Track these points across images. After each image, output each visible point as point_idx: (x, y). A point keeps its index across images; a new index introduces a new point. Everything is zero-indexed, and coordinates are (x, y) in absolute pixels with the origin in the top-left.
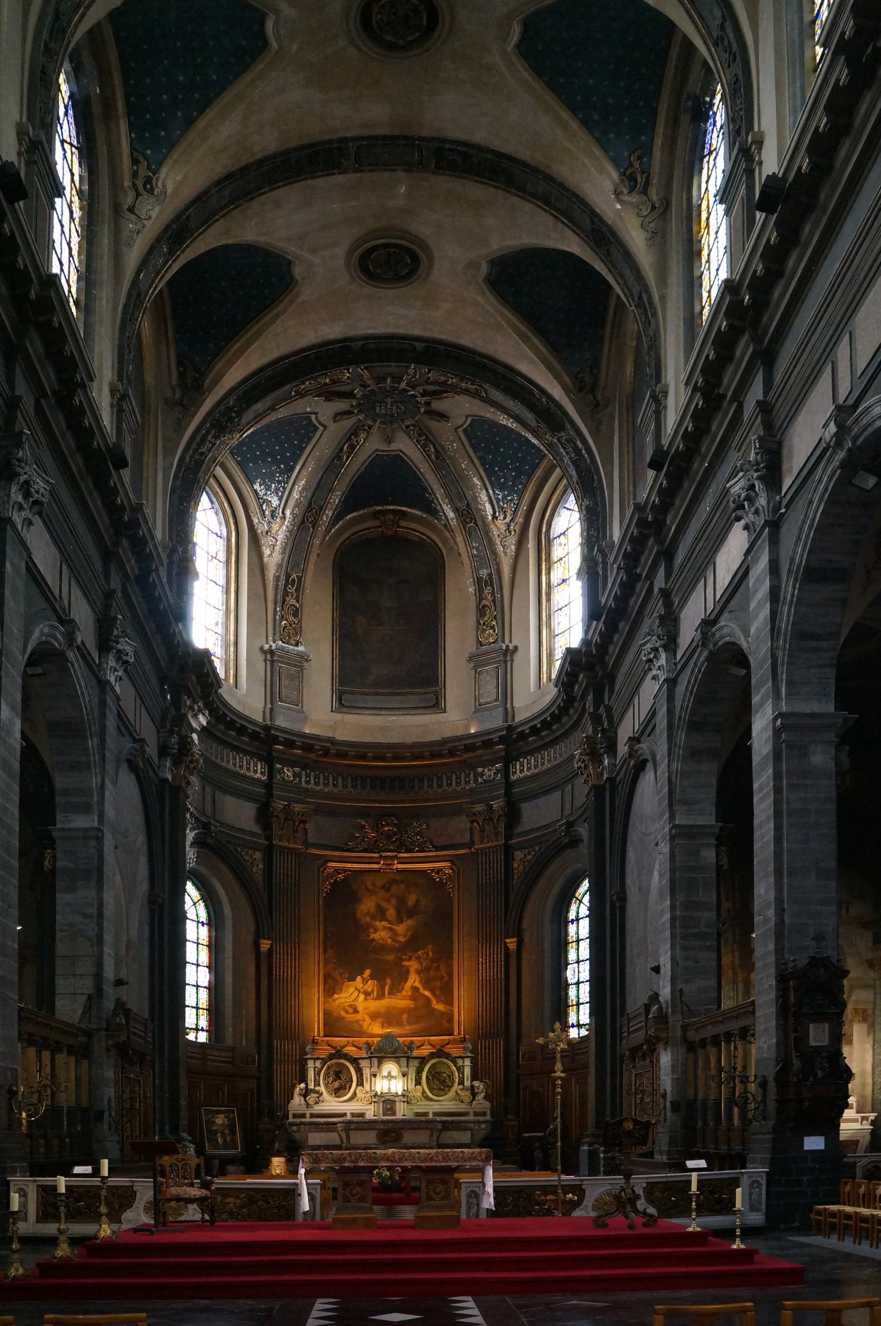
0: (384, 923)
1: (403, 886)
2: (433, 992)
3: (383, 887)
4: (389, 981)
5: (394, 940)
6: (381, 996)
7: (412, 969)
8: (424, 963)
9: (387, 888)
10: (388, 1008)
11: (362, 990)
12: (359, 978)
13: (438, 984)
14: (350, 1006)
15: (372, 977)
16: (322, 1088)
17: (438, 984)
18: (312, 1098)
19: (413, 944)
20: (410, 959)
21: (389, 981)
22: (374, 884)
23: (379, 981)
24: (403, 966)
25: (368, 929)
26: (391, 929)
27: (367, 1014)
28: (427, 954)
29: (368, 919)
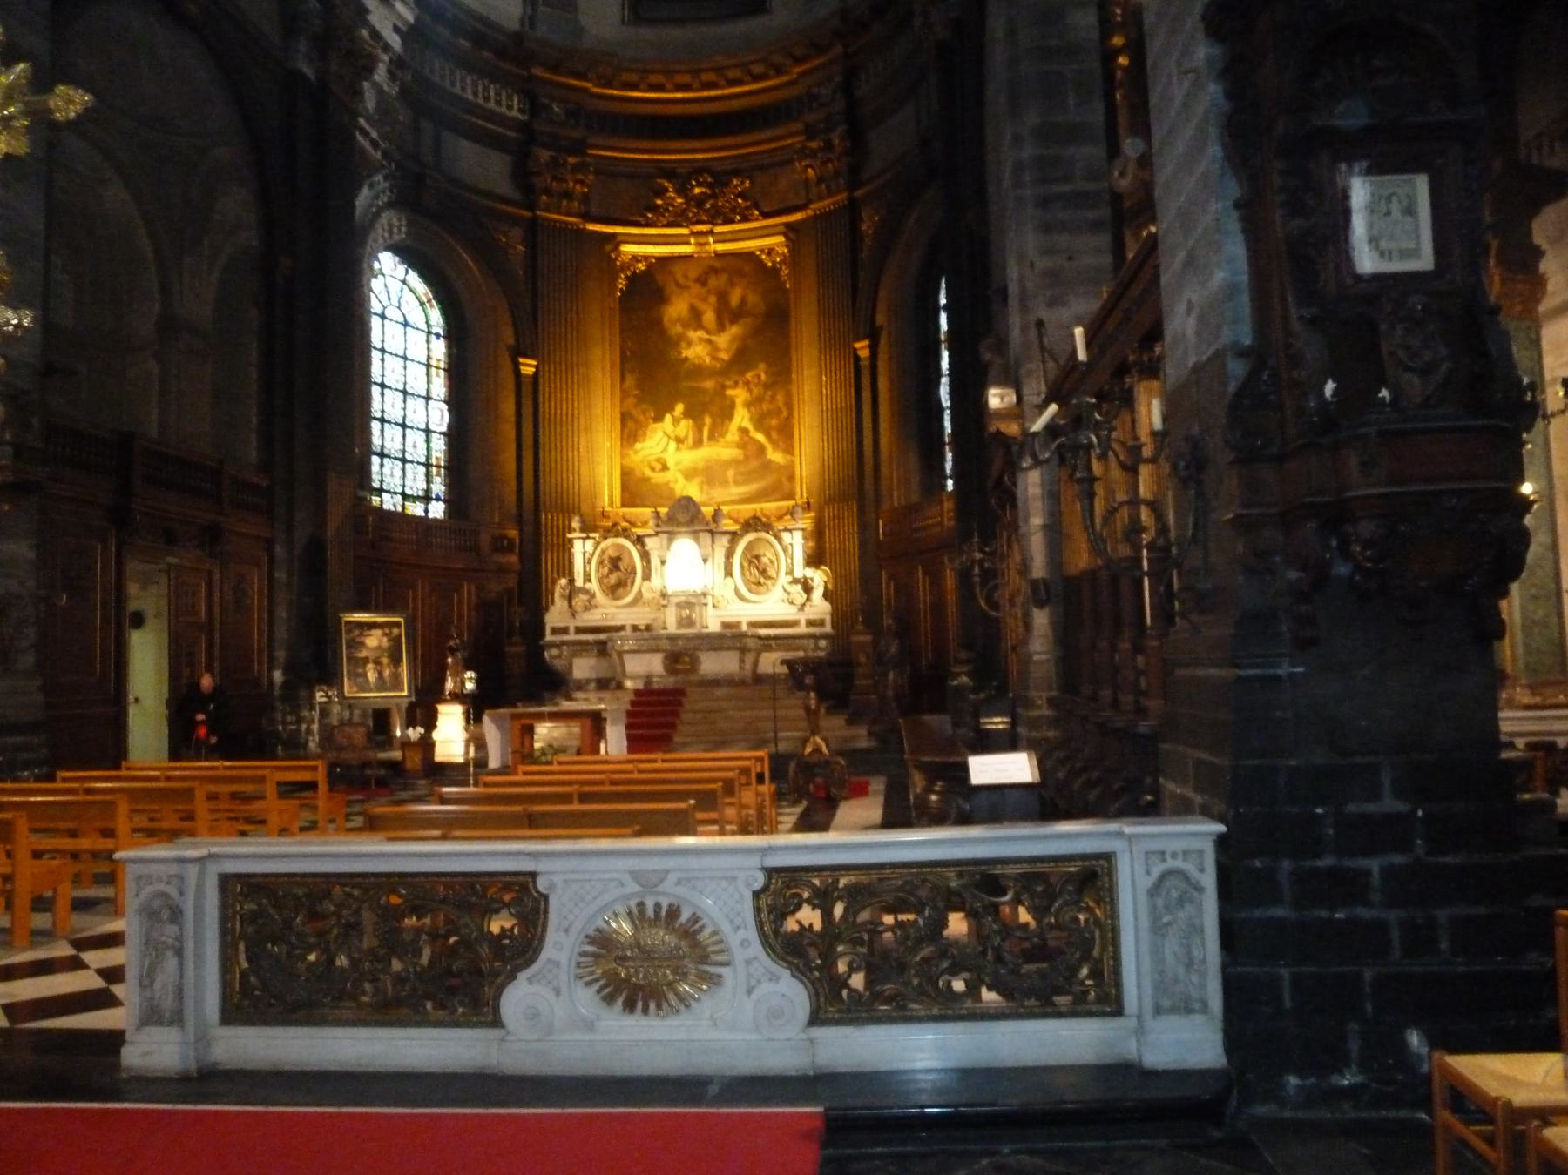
0: (701, 334)
1: (724, 277)
2: (768, 435)
3: (698, 280)
4: (708, 420)
5: (714, 358)
6: (698, 443)
7: (739, 401)
8: (756, 391)
9: (702, 281)
10: (708, 461)
11: (672, 435)
12: (668, 418)
13: (774, 422)
14: (658, 460)
15: (687, 414)
16: (594, 586)
17: (774, 422)
18: (578, 602)
19: (741, 361)
20: (736, 383)
21: (708, 420)
22: (686, 277)
23: (694, 419)
24: (724, 396)
25: (677, 344)
26: (709, 342)
27: (680, 471)
28: (759, 376)
29: (678, 329)
